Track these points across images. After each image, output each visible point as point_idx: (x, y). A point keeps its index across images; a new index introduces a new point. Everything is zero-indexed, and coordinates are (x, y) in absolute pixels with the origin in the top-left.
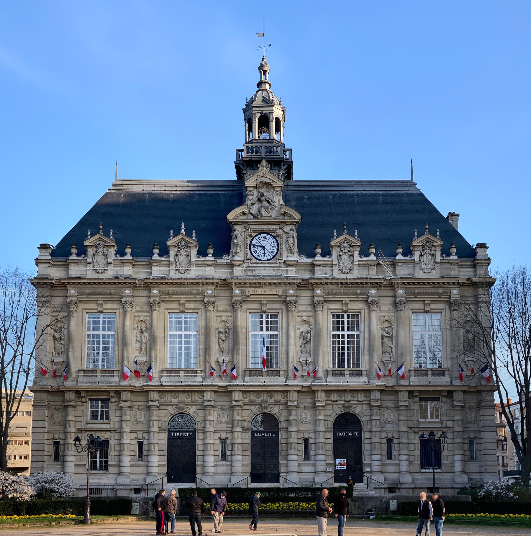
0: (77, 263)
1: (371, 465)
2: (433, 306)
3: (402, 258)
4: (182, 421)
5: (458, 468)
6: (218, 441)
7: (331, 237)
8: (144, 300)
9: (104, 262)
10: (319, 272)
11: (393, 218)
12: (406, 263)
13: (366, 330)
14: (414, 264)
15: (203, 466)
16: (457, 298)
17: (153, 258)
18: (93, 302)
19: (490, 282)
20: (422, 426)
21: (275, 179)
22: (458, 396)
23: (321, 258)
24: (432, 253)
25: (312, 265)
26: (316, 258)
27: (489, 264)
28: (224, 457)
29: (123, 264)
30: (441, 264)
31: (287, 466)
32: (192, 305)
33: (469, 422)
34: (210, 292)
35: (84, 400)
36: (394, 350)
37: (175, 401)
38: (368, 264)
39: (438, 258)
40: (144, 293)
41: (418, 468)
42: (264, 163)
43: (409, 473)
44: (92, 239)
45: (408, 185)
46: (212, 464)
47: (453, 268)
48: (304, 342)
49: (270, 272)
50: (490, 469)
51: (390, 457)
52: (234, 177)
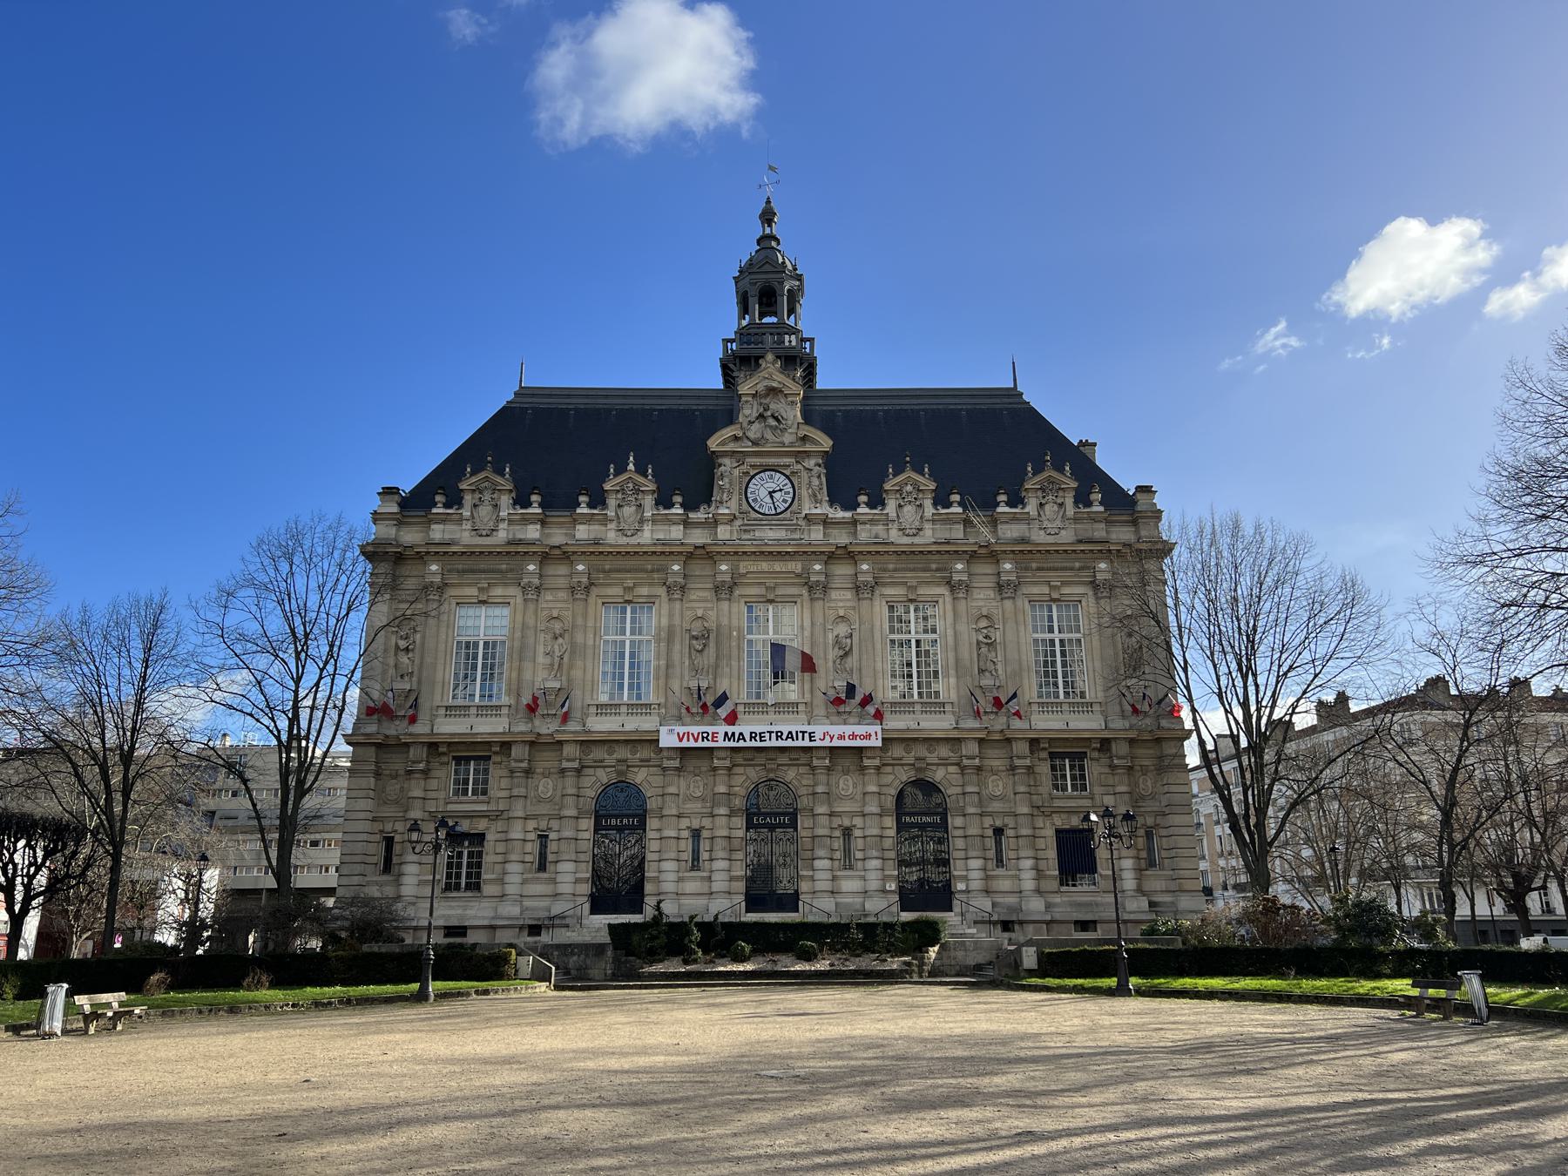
0: (444, 519)
1: (965, 879)
2: (1066, 590)
3: (1007, 509)
4: (622, 796)
5: (1129, 882)
6: (686, 834)
7: (884, 477)
8: (562, 582)
9: (492, 517)
10: (864, 534)
11: (987, 447)
12: (1014, 519)
13: (950, 632)
14: (1027, 519)
15: (657, 880)
16: (1108, 576)
17: (579, 511)
18: (469, 585)
19: (1166, 549)
20: (1057, 803)
21: (789, 382)
22: (1121, 749)
23: (867, 510)
24: (1059, 501)
25: (854, 522)
26: (859, 510)
27: (1159, 518)
28: (695, 864)
29: (526, 520)
30: (1076, 520)
31: (812, 879)
32: (644, 591)
33: (1143, 798)
34: (676, 568)
35: (445, 759)
36: (1000, 667)
37: (610, 760)
38: (948, 520)
39: (1070, 510)
40: (562, 570)
41: (1055, 884)
42: (770, 357)
43: (1038, 892)
44: (474, 479)
45: (1009, 396)
46: (672, 877)
47: (1097, 526)
48: (841, 653)
49: (781, 534)
50: (1188, 885)
51: (1000, 862)
52: (718, 383)
